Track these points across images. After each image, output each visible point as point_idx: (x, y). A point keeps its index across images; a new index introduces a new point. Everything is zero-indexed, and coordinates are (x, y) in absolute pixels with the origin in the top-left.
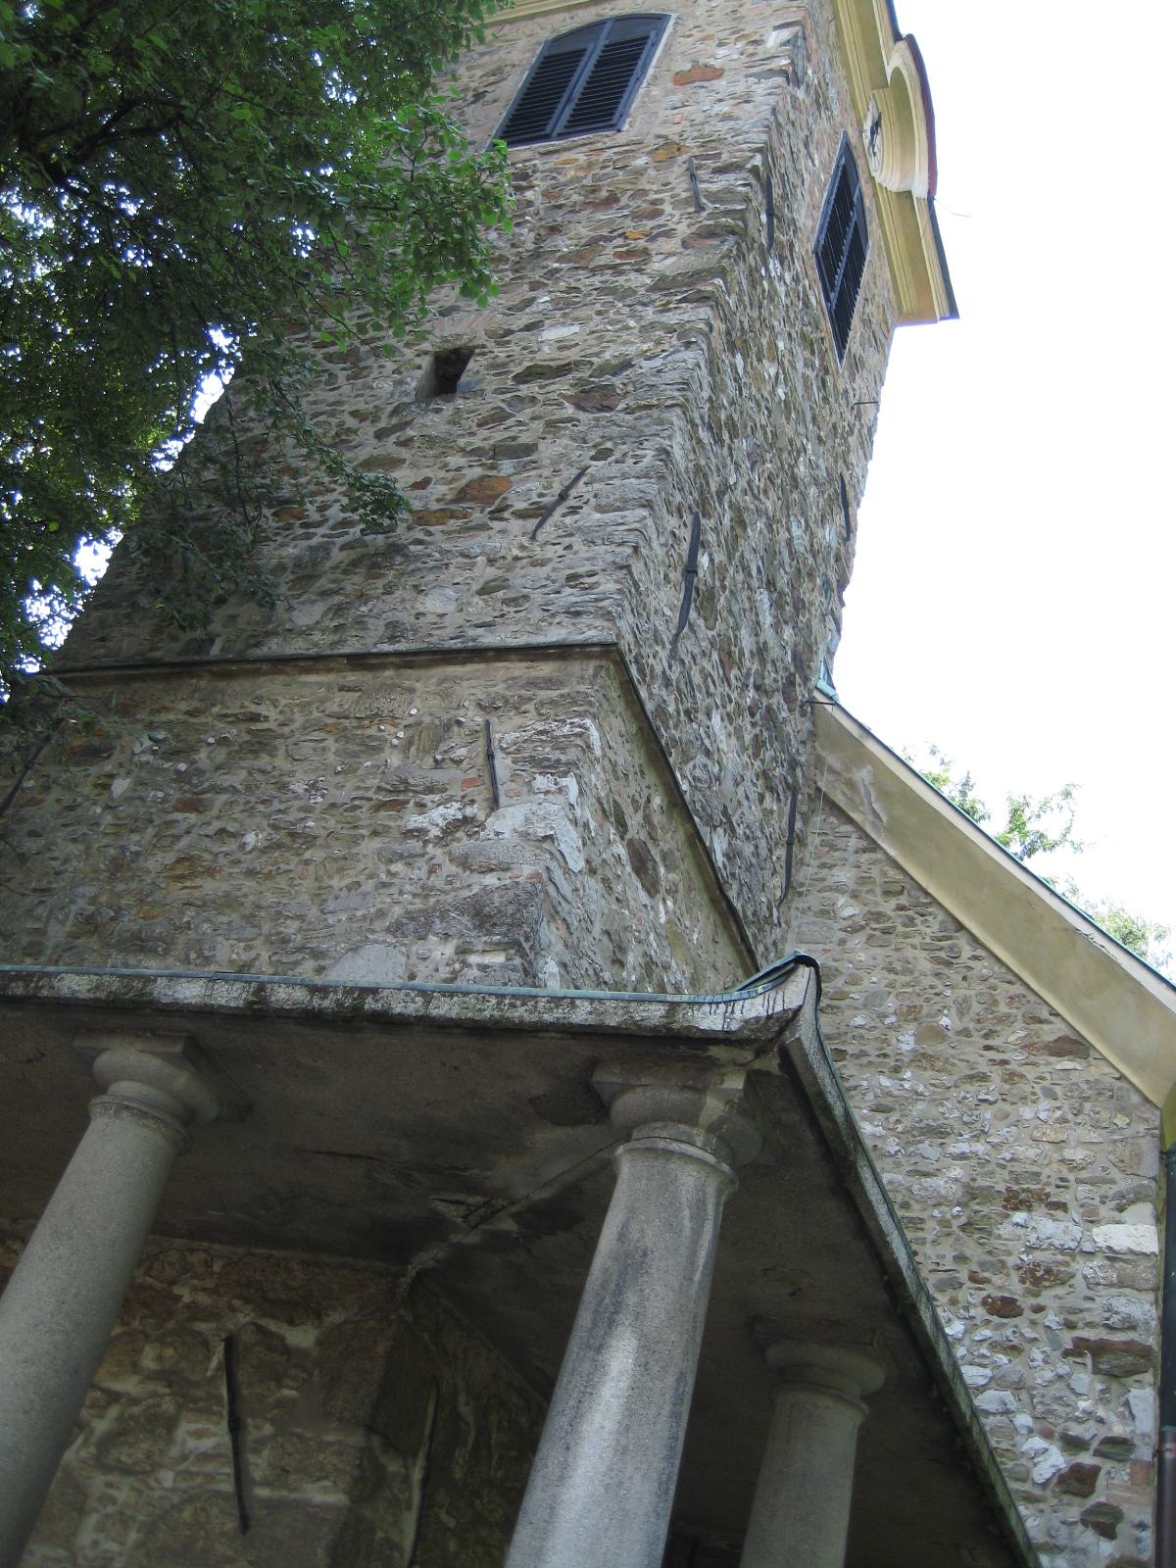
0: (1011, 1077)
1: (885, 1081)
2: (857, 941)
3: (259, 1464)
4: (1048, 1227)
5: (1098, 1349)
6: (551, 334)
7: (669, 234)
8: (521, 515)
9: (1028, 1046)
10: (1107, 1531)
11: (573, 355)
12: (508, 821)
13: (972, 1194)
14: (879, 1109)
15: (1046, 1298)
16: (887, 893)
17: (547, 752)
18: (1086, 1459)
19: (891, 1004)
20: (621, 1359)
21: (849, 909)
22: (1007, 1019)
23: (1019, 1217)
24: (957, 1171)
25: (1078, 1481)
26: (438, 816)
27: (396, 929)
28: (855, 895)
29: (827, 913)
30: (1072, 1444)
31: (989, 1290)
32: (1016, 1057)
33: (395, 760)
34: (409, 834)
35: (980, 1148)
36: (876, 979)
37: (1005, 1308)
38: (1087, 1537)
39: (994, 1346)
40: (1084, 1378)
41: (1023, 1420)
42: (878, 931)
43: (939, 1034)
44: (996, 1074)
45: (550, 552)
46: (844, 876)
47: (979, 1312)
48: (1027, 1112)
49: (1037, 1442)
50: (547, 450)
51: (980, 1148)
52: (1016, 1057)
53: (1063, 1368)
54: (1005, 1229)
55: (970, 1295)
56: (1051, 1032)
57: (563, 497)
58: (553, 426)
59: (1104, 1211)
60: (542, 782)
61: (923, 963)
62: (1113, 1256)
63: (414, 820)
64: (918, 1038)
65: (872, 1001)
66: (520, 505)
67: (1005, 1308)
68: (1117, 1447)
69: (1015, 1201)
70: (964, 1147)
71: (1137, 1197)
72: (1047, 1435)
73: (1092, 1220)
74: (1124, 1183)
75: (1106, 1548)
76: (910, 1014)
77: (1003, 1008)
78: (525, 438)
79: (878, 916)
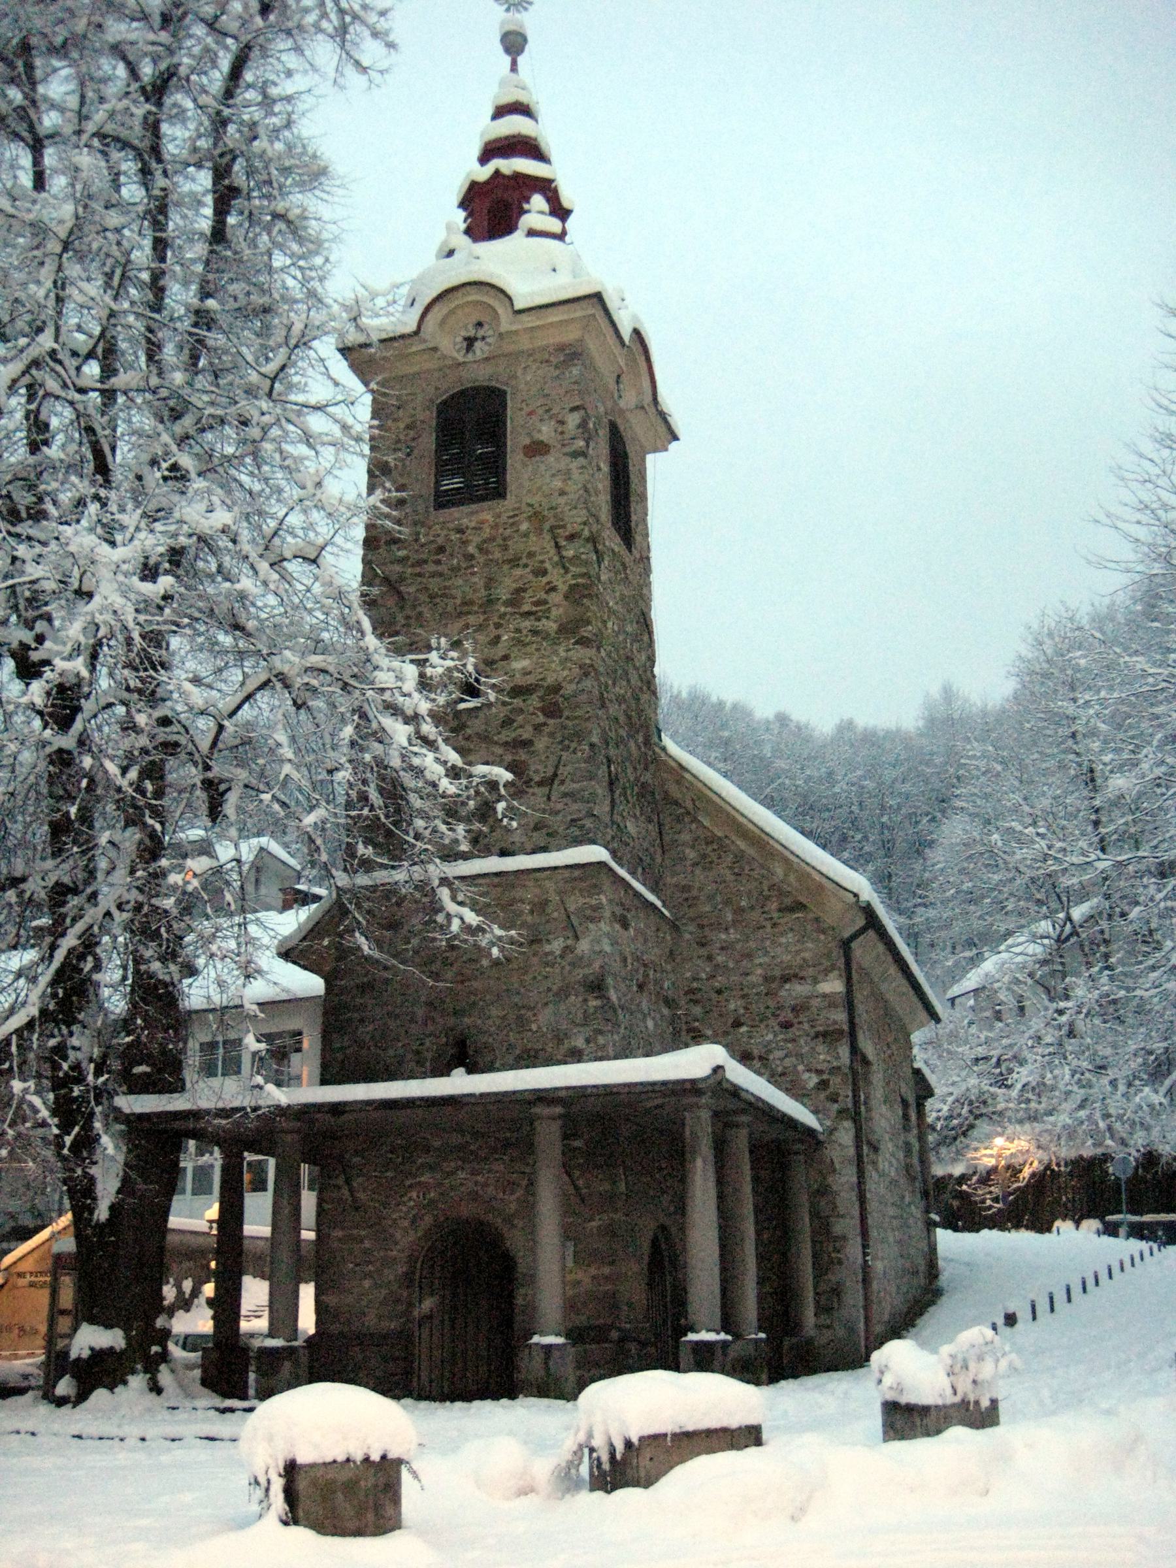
0: (774, 925)
1: (723, 936)
2: (698, 871)
3: (581, 1183)
4: (799, 989)
5: (825, 1034)
6: (518, 665)
7: (554, 589)
8: (540, 784)
9: (780, 910)
10: (836, 1101)
11: (530, 680)
12: (584, 946)
13: (767, 979)
14: (722, 948)
15: (802, 1018)
16: (707, 844)
17: (588, 912)
18: (825, 1077)
19: (719, 898)
20: (699, 1162)
21: (691, 854)
22: (768, 898)
23: (787, 986)
24: (759, 971)
25: (823, 1085)
26: (557, 946)
27: (556, 994)
28: (693, 847)
29: (683, 859)
30: (819, 1072)
31: (781, 1018)
32: (775, 915)
33: (529, 919)
34: (547, 954)
35: (766, 959)
36: (711, 888)
37: (786, 1025)
38: (828, 1104)
39: (785, 1040)
40: (821, 1048)
41: (801, 1068)
42: (704, 862)
43: (742, 910)
44: (768, 924)
45: (559, 806)
46: (685, 837)
47: (777, 1028)
48: (783, 940)
49: (806, 1076)
50: (541, 744)
51: (766, 959)
52: (775, 915)
53: (812, 1044)
54: (783, 993)
55: (773, 1022)
56: (788, 901)
57: (555, 775)
58: (538, 728)
59: (820, 977)
60: (591, 926)
61: (730, 877)
62: (825, 996)
63: (547, 948)
64: (735, 912)
65: (711, 898)
66: (537, 778)
67: (786, 1025)
68: (835, 1070)
69: (786, 979)
70: (757, 961)
71: (833, 967)
72: (809, 1070)
73: (816, 981)
74: (827, 963)
75: (836, 1106)
76: (727, 902)
77: (766, 893)
78: (526, 736)
79: (704, 856)
